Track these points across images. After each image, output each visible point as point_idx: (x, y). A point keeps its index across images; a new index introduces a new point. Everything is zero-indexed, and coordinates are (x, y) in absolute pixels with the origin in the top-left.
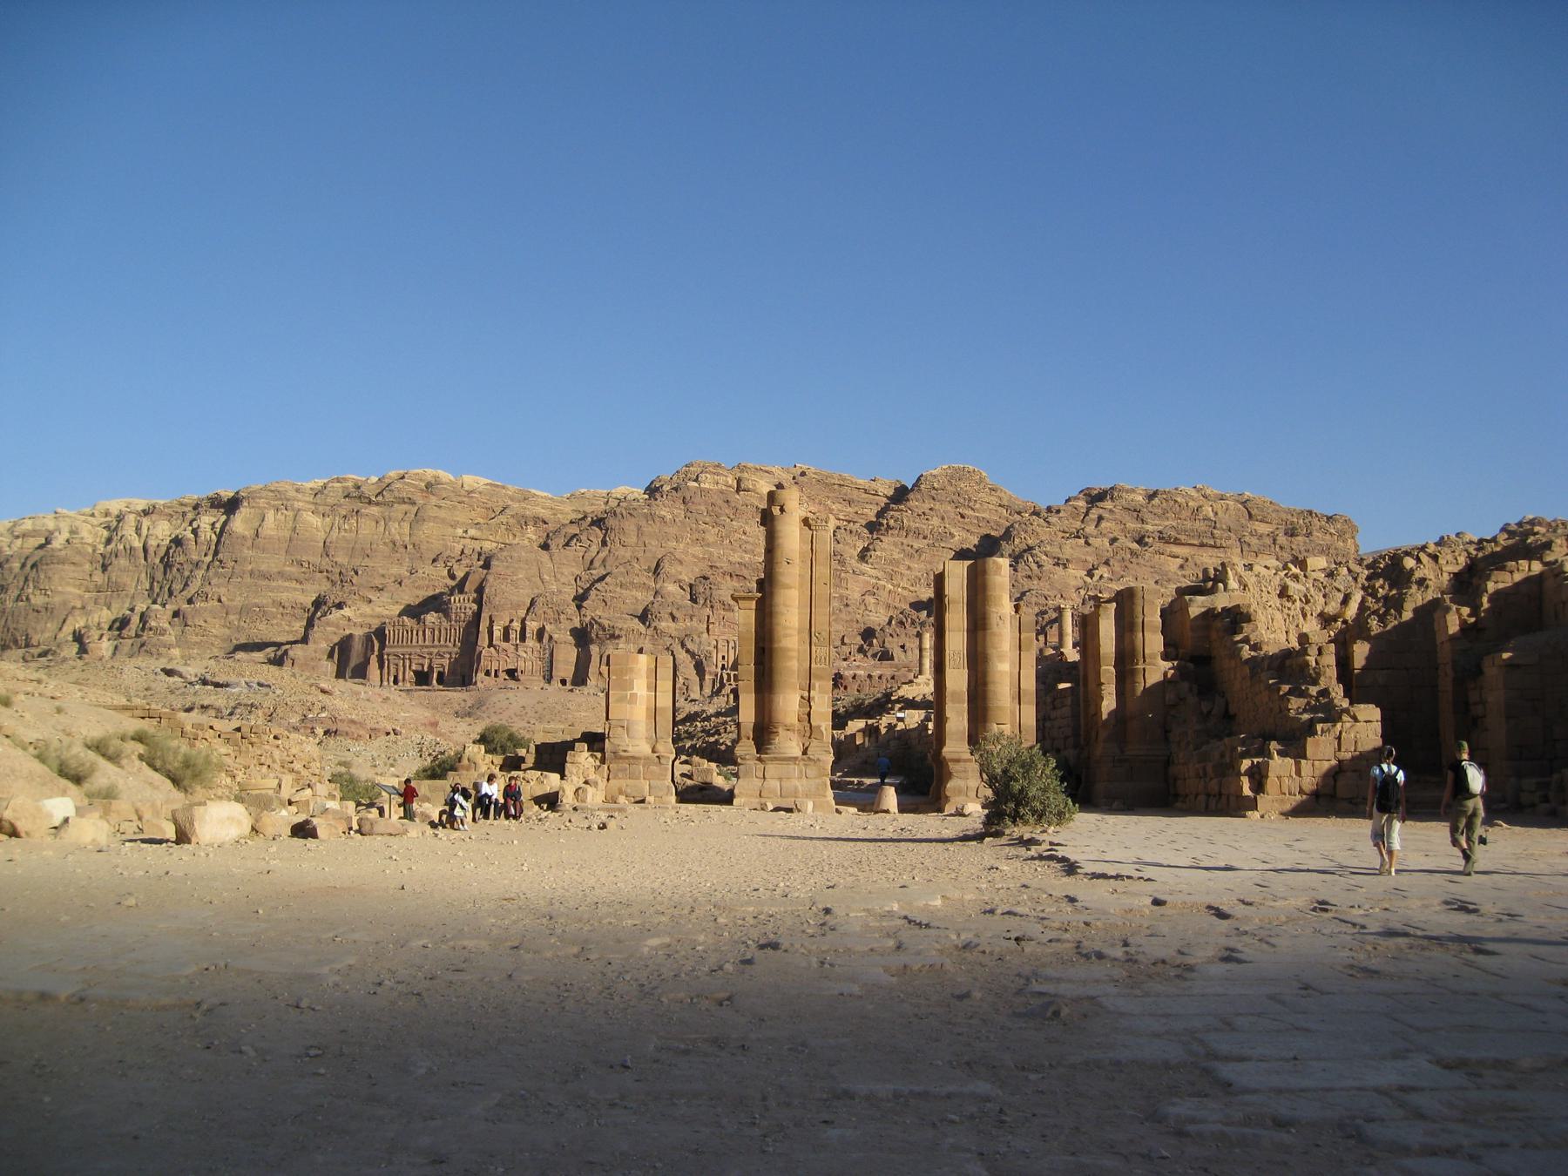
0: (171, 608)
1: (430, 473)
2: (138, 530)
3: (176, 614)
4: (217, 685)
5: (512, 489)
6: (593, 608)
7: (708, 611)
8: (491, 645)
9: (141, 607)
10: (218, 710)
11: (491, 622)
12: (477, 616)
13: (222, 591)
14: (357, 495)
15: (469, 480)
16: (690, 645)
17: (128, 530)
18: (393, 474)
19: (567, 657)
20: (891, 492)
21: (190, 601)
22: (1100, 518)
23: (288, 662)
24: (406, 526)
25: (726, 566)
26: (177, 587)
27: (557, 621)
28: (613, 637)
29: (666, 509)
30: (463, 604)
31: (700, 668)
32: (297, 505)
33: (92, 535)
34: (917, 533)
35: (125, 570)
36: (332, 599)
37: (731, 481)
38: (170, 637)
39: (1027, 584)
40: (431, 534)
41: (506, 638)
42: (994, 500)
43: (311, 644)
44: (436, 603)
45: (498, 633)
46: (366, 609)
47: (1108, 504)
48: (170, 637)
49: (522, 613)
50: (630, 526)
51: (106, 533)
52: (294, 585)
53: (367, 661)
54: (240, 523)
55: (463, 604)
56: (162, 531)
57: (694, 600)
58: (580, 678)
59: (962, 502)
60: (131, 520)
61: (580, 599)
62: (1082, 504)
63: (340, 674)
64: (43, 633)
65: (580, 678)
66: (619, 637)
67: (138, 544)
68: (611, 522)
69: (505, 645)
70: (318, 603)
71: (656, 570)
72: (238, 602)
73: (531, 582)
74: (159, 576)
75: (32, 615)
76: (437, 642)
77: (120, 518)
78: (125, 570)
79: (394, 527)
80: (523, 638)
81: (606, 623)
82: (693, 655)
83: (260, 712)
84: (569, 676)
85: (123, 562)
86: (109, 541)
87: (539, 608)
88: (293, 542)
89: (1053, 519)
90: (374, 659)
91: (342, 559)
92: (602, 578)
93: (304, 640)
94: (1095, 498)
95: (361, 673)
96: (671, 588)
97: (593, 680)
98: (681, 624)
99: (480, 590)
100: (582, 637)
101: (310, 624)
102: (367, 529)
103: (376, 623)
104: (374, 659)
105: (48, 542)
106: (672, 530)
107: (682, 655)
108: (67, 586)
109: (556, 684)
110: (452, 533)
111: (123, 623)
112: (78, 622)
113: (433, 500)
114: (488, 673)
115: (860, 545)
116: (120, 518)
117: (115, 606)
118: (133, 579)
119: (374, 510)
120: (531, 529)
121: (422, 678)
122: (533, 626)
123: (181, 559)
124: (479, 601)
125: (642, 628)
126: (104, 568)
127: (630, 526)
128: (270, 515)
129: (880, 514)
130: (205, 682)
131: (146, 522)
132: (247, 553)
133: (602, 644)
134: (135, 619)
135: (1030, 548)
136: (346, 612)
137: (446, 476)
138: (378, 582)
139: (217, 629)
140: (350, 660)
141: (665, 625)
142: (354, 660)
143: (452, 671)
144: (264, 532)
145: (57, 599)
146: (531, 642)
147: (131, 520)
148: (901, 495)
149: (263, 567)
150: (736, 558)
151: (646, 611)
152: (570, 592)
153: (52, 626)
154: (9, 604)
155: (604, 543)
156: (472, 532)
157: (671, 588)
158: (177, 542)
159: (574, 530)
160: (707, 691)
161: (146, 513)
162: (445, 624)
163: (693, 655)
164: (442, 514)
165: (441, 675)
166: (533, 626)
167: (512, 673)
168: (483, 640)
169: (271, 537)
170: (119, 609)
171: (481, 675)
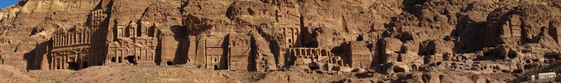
7: (276, 8)
8: (116, 39)
11: (116, 22)
12: (107, 20)
16: (265, 30)
19: (171, 46)
27: (165, 20)
58: (181, 58)
65: (181, 58)
66: (210, 27)
69: (127, 39)
80: (139, 34)
81: (200, 17)
97: (192, 61)
104: (45, 57)
107: (259, 39)
114: (114, 60)
122: (147, 24)
125: (228, 20)
141: (245, 16)
144: (35, 11)
146: (144, 36)
160: (282, 63)
168: (110, 37)
169: (39, 13)
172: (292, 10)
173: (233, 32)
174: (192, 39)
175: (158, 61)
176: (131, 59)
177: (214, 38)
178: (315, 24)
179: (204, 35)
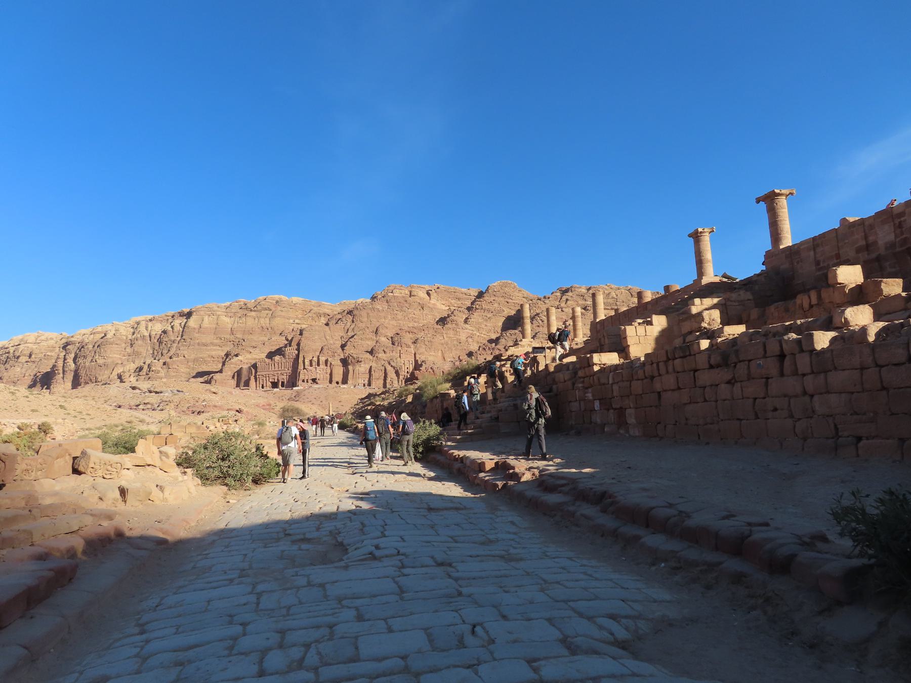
0: (162, 361)
1: (277, 297)
2: (147, 328)
3: (164, 364)
4: (156, 393)
5: (313, 302)
6: (349, 350)
7: (399, 348)
9: (148, 362)
10: (152, 405)
12: (298, 356)
13: (185, 352)
14: (245, 308)
15: (295, 299)
16: (392, 364)
17: (142, 328)
18: (261, 298)
20: (476, 294)
21: (171, 358)
22: (567, 300)
23: (213, 382)
24: (267, 320)
25: (406, 328)
26: (165, 352)
27: (334, 356)
28: (358, 361)
29: (378, 305)
30: (291, 351)
31: (397, 373)
32: (218, 313)
33: (125, 331)
34: (489, 311)
35: (141, 346)
36: (233, 353)
37: (407, 292)
38: (162, 374)
39: (538, 329)
40: (278, 322)
41: (311, 365)
42: (520, 295)
43: (224, 373)
44: (279, 352)
45: (307, 363)
46: (249, 356)
47: (570, 294)
48: (162, 374)
49: (318, 354)
50: (364, 313)
51: (132, 330)
52: (218, 348)
53: (249, 379)
54: (192, 322)
55: (291, 351)
56: (158, 328)
57: (393, 344)
58: (345, 381)
59: (507, 297)
60: (143, 324)
61: (343, 347)
62: (559, 294)
63: (238, 385)
64: (103, 376)
67: (147, 334)
68: (355, 312)
70: (227, 355)
71: (376, 332)
72: (193, 356)
73: (321, 340)
74: (157, 347)
75: (98, 368)
76: (281, 368)
77: (138, 323)
78: (141, 346)
79: (262, 321)
80: (318, 365)
81: (355, 356)
82: (394, 368)
83: (172, 405)
84: (340, 381)
85: (140, 342)
86: (134, 333)
87: (325, 351)
88: (217, 330)
89: (547, 301)
90: (252, 378)
91: (239, 336)
92: (353, 337)
93: (221, 371)
94: (564, 292)
95: (247, 384)
96: (383, 339)
98: (388, 355)
99: (298, 345)
100: (345, 362)
101: (224, 364)
102: (250, 322)
103: (253, 362)
104: (252, 378)
105: (105, 335)
106: (382, 314)
107: (389, 368)
108: (114, 354)
109: (334, 384)
110: (288, 322)
111: (141, 369)
112: (119, 370)
113: (279, 308)
114: (303, 381)
115: (464, 317)
116: (138, 323)
117: (137, 362)
118: (145, 350)
119: (253, 314)
120: (322, 318)
121: (275, 385)
122: (322, 359)
123: (167, 339)
124: (298, 349)
125: (371, 357)
126: (132, 345)
127: (364, 313)
128: (206, 318)
129: (472, 303)
130: (150, 392)
131: (150, 324)
132: (197, 335)
133: (354, 365)
134: (146, 367)
135: (538, 314)
136: (240, 358)
137: (284, 298)
138: (254, 344)
139: (183, 369)
140: (241, 380)
142: (244, 379)
143: (288, 382)
145: (110, 360)
146: (322, 366)
147: (143, 324)
148: (481, 295)
149: (204, 341)
150: (411, 325)
151: (372, 349)
152: (339, 343)
153: (107, 372)
154: (87, 364)
155: (353, 322)
156: (297, 321)
157: (383, 339)
158: (165, 332)
159: (340, 316)
161: (151, 320)
162: (284, 360)
163: (394, 368)
164: (283, 314)
165: (283, 383)
166: (322, 359)
167: (314, 380)
168: (301, 366)
169: (207, 328)
170: (139, 363)
171: (300, 382)
172: (409, 349)
173: (374, 365)
174: (350, 368)
175: (331, 382)
176: (314, 380)
177: (363, 368)
178: (423, 358)
179: (357, 367)
